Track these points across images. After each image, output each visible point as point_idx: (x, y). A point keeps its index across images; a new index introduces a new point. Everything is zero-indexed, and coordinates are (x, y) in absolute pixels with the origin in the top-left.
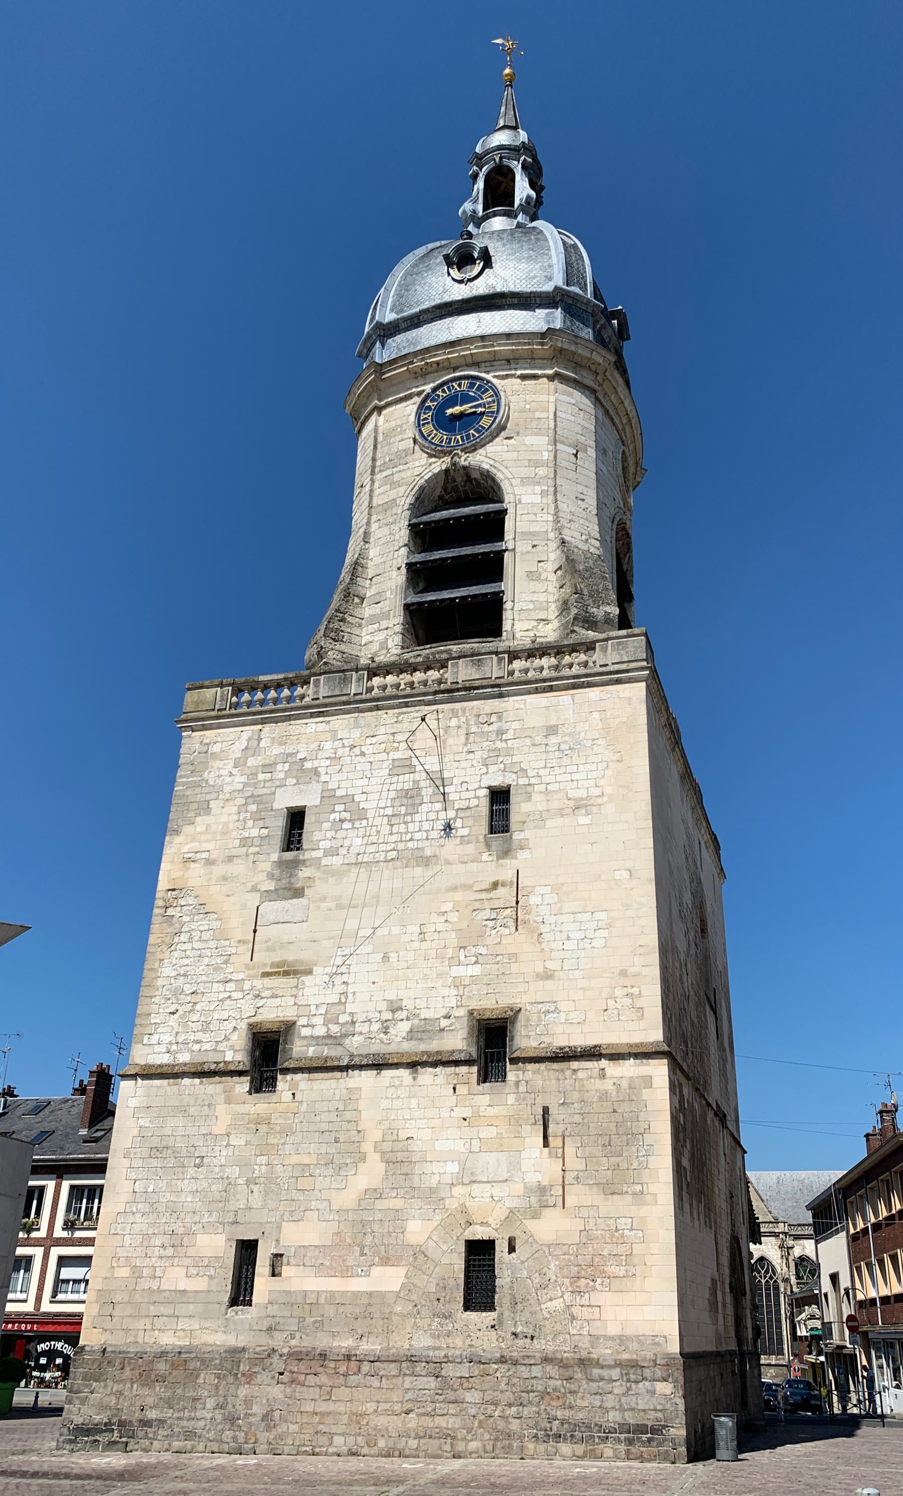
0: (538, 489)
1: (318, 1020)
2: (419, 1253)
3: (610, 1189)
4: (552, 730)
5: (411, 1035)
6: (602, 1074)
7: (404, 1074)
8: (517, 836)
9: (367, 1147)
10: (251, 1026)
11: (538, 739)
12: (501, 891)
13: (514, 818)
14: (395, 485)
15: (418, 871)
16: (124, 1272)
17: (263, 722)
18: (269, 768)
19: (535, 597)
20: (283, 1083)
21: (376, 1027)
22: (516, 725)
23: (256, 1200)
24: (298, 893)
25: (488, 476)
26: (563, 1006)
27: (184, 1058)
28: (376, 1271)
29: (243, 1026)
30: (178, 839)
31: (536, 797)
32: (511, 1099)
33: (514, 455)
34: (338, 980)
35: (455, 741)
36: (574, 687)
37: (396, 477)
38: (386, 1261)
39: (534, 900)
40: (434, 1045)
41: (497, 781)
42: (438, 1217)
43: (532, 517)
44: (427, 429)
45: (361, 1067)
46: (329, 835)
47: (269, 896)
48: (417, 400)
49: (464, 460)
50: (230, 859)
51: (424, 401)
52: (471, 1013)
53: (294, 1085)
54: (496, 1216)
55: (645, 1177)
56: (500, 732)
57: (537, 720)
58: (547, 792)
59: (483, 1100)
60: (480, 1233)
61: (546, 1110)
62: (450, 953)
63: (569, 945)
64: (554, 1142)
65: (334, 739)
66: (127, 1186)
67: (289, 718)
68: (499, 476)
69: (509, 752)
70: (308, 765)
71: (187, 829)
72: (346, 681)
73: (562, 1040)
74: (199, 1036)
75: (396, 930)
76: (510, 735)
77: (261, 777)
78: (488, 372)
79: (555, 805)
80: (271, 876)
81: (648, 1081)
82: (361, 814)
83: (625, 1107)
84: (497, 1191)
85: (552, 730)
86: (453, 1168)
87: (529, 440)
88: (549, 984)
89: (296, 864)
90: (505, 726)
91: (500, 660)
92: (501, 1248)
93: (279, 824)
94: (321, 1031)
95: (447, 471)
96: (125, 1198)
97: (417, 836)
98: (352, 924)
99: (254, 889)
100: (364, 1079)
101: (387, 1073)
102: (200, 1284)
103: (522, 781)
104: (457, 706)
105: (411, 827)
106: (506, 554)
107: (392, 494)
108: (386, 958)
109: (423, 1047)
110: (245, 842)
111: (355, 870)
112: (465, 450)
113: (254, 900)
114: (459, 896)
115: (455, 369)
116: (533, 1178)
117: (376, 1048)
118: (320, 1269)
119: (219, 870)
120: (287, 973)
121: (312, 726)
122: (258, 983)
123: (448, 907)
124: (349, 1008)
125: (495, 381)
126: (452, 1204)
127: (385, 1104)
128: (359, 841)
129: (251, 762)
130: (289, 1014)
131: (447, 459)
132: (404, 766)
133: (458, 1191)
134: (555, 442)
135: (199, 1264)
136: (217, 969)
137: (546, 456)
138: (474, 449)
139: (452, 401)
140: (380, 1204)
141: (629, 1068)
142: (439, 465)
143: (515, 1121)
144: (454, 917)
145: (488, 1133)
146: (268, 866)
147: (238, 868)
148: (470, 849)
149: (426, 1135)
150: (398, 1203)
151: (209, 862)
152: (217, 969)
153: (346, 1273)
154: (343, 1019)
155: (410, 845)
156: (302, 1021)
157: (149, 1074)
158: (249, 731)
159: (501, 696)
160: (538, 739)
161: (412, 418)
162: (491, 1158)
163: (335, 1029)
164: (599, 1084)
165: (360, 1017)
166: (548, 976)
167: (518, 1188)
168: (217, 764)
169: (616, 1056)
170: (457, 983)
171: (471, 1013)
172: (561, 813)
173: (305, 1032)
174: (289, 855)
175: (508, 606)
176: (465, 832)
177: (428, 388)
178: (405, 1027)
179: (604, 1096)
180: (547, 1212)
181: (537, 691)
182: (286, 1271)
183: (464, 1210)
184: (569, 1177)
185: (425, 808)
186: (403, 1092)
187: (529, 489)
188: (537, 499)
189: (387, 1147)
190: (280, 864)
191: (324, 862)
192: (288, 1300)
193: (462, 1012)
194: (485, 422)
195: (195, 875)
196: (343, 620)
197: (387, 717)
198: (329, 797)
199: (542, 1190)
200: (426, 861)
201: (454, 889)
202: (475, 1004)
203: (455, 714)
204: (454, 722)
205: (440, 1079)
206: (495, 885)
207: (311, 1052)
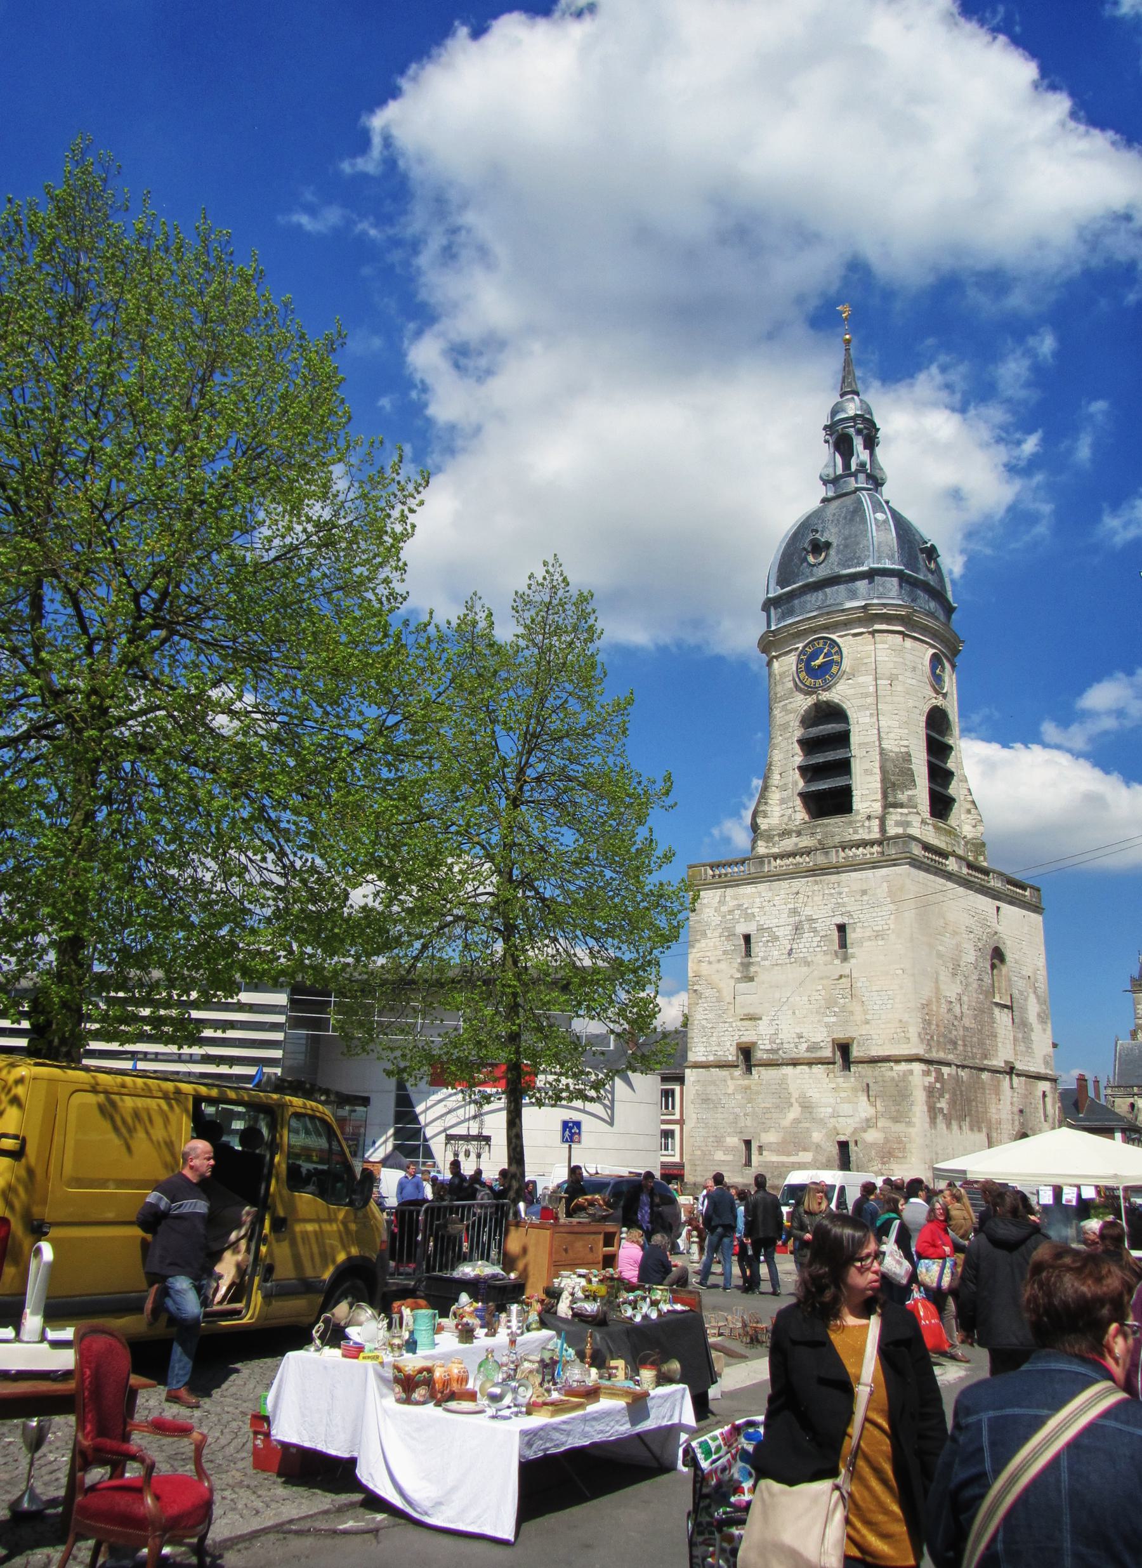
0: (868, 713)
1: (767, 1042)
2: (818, 1146)
3: (896, 1120)
4: (864, 892)
5: (808, 1050)
6: (892, 1068)
7: (805, 1068)
8: (850, 951)
9: (793, 1100)
10: (738, 1044)
11: (858, 898)
12: (843, 980)
13: (848, 941)
14: (788, 712)
15: (805, 969)
16: (699, 1153)
17: (726, 887)
18: (731, 912)
19: (870, 786)
20: (754, 1070)
21: (792, 1045)
22: (846, 889)
23: (749, 1123)
24: (751, 979)
25: (838, 705)
26: (875, 1037)
27: (711, 1058)
28: (801, 1154)
29: (734, 1043)
30: (695, 950)
31: (858, 930)
32: (852, 1079)
33: (852, 691)
34: (774, 1023)
35: (818, 898)
36: (874, 868)
37: (789, 707)
38: (805, 1150)
39: (860, 984)
40: (819, 1054)
41: (839, 920)
42: (824, 1131)
43: (864, 733)
44: (803, 675)
45: (787, 1065)
46: (763, 949)
47: (739, 980)
48: (797, 653)
49: (825, 696)
50: (719, 961)
51: (799, 656)
52: (833, 1040)
53: (759, 1072)
54: (849, 1131)
55: (911, 1114)
56: (841, 893)
57: (856, 886)
58: (863, 927)
59: (841, 1080)
60: (843, 1138)
61: (868, 1085)
62: (822, 1010)
63: (876, 1007)
64: (872, 1099)
65: (760, 897)
66: (694, 1116)
67: (737, 885)
68: (844, 706)
69: (844, 905)
70: (749, 911)
71: (698, 945)
72: (762, 863)
73: (875, 1052)
74: (716, 1048)
75: (798, 999)
76: (844, 895)
77: (729, 917)
78: (834, 633)
79: (868, 934)
80: (738, 970)
81: (911, 1072)
82: (777, 938)
83: (901, 1084)
84: (850, 1121)
85: (864, 892)
86: (830, 1110)
87: (861, 679)
88: (867, 1026)
89: (749, 964)
90: (842, 890)
91: (837, 851)
92: (852, 1146)
93: (742, 942)
94: (768, 1047)
95: (815, 704)
96: (694, 1120)
97: (804, 950)
98: (777, 996)
99: (732, 977)
100: (788, 1070)
101: (799, 1067)
102: (729, 1158)
103: (851, 921)
104: (818, 878)
105: (801, 946)
106: (852, 759)
107: (787, 718)
108: (794, 1013)
109: (814, 1055)
110: (725, 952)
111: (776, 968)
112: (824, 690)
113: (732, 982)
114: (825, 982)
115: (815, 632)
116: (863, 1115)
117: (793, 1055)
118: (779, 1152)
119: (716, 966)
120: (751, 1019)
121: (749, 890)
122: (739, 1023)
123: (820, 987)
124: (780, 1036)
125: (838, 640)
126: (830, 1126)
127: (799, 1081)
128: (776, 953)
129: (724, 909)
130: (753, 1039)
131: (814, 696)
132: (794, 912)
133: (833, 1120)
134: (876, 679)
135: (727, 1150)
136: (720, 1016)
137: (872, 689)
138: (828, 689)
139: (814, 656)
140: (800, 1125)
141: (903, 1066)
142: (810, 701)
143: (855, 1090)
144: (823, 992)
145: (843, 1095)
146: (736, 965)
147: (723, 966)
148: (828, 958)
149: (817, 1095)
150: (807, 1125)
151: (710, 963)
152: (720, 1016)
153: (789, 1155)
154: (778, 1041)
155: (801, 955)
156: (760, 1042)
157: (697, 1066)
158: (719, 892)
159: (838, 873)
160: (858, 898)
161: (794, 668)
162: (846, 1105)
163: (775, 1046)
164: (890, 1073)
165: (785, 1041)
166: (867, 1022)
167: (857, 1120)
168: (708, 910)
169: (897, 1060)
170: (827, 1025)
171: (833, 1040)
172: (869, 939)
173: (762, 1047)
174: (746, 960)
175: (854, 793)
176: (825, 948)
177: (800, 645)
178: (804, 1046)
179: (893, 1079)
180: (870, 1130)
181: (855, 870)
182: (764, 1153)
183: (835, 1128)
184: (879, 1115)
185: (806, 935)
186: (806, 1076)
187: (862, 714)
188: (867, 720)
189: (801, 1100)
190: (742, 964)
191: (762, 963)
192: (766, 1164)
193: (829, 1039)
194: (834, 669)
195: (705, 969)
196: (766, 803)
197: (784, 884)
198: (761, 929)
199: (868, 1120)
200: (808, 964)
201: (822, 978)
202: (835, 1036)
203: (816, 882)
204: (816, 888)
205: (821, 1071)
206: (841, 977)
207: (765, 1056)
